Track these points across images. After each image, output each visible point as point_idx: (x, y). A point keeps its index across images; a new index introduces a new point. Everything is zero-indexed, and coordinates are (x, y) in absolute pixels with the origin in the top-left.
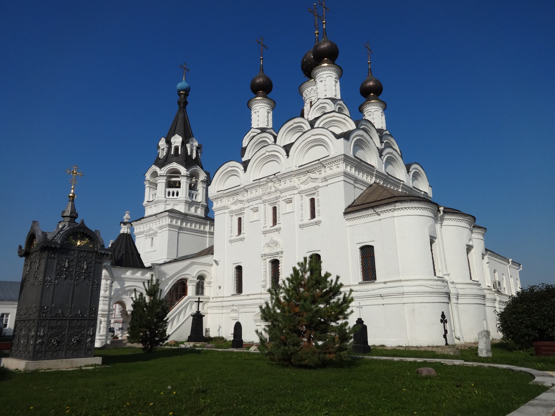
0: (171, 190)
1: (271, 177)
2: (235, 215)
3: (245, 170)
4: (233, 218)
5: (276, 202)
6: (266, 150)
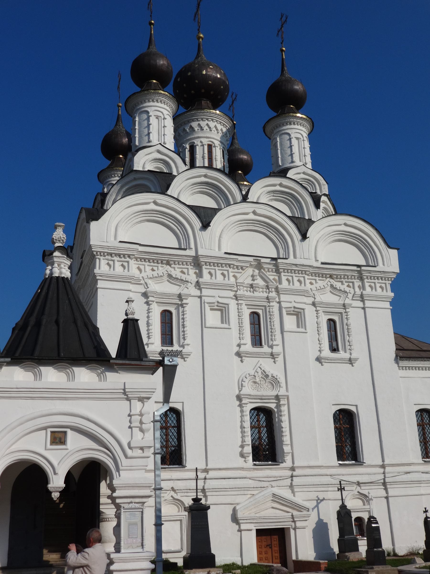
1: (263, 260)
3: (205, 226)
4: (152, 307)
5: (265, 306)
6: (252, 210)
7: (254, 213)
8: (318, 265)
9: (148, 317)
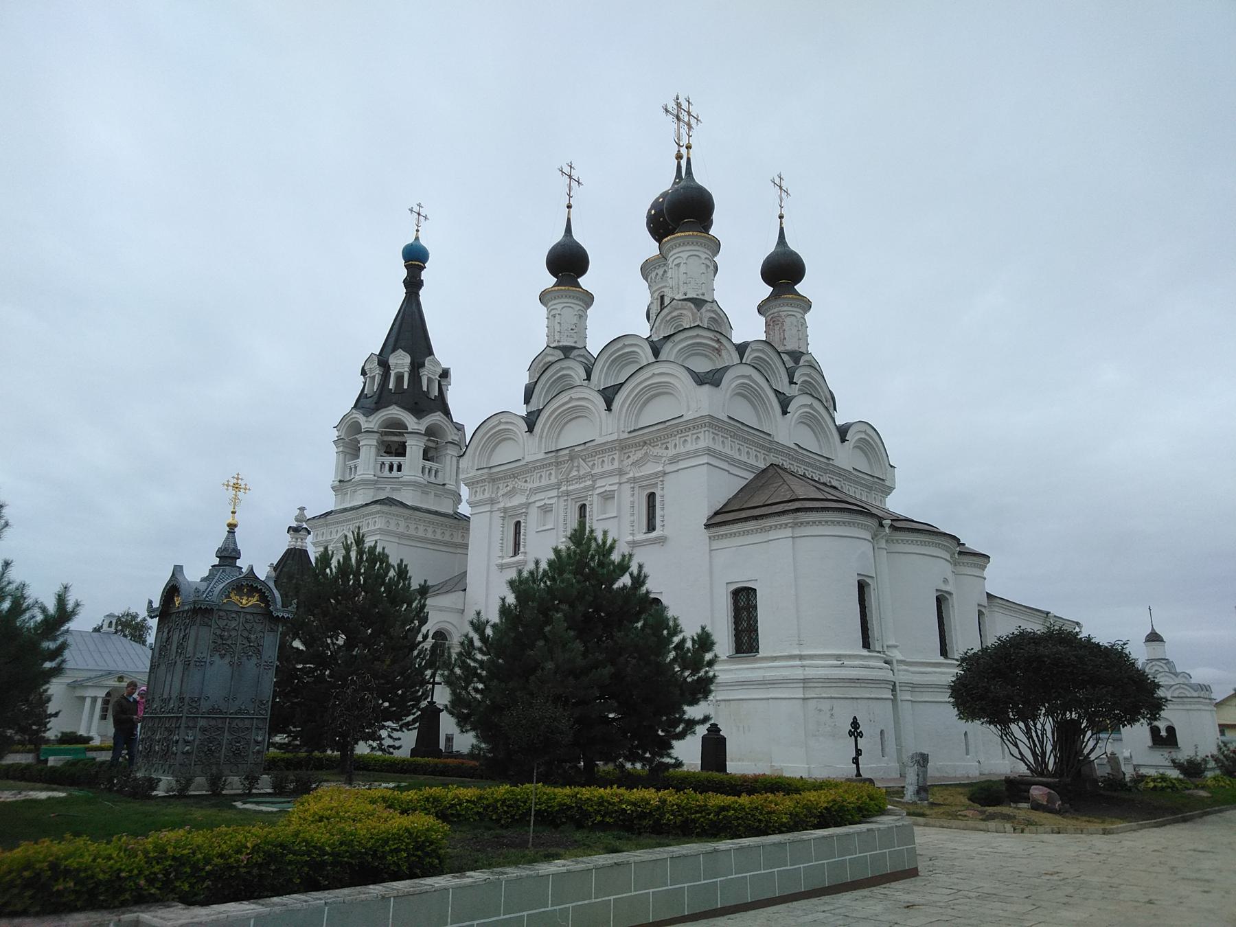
0: (388, 459)
1: (577, 449)
6: (569, 396)
8: (626, 435)
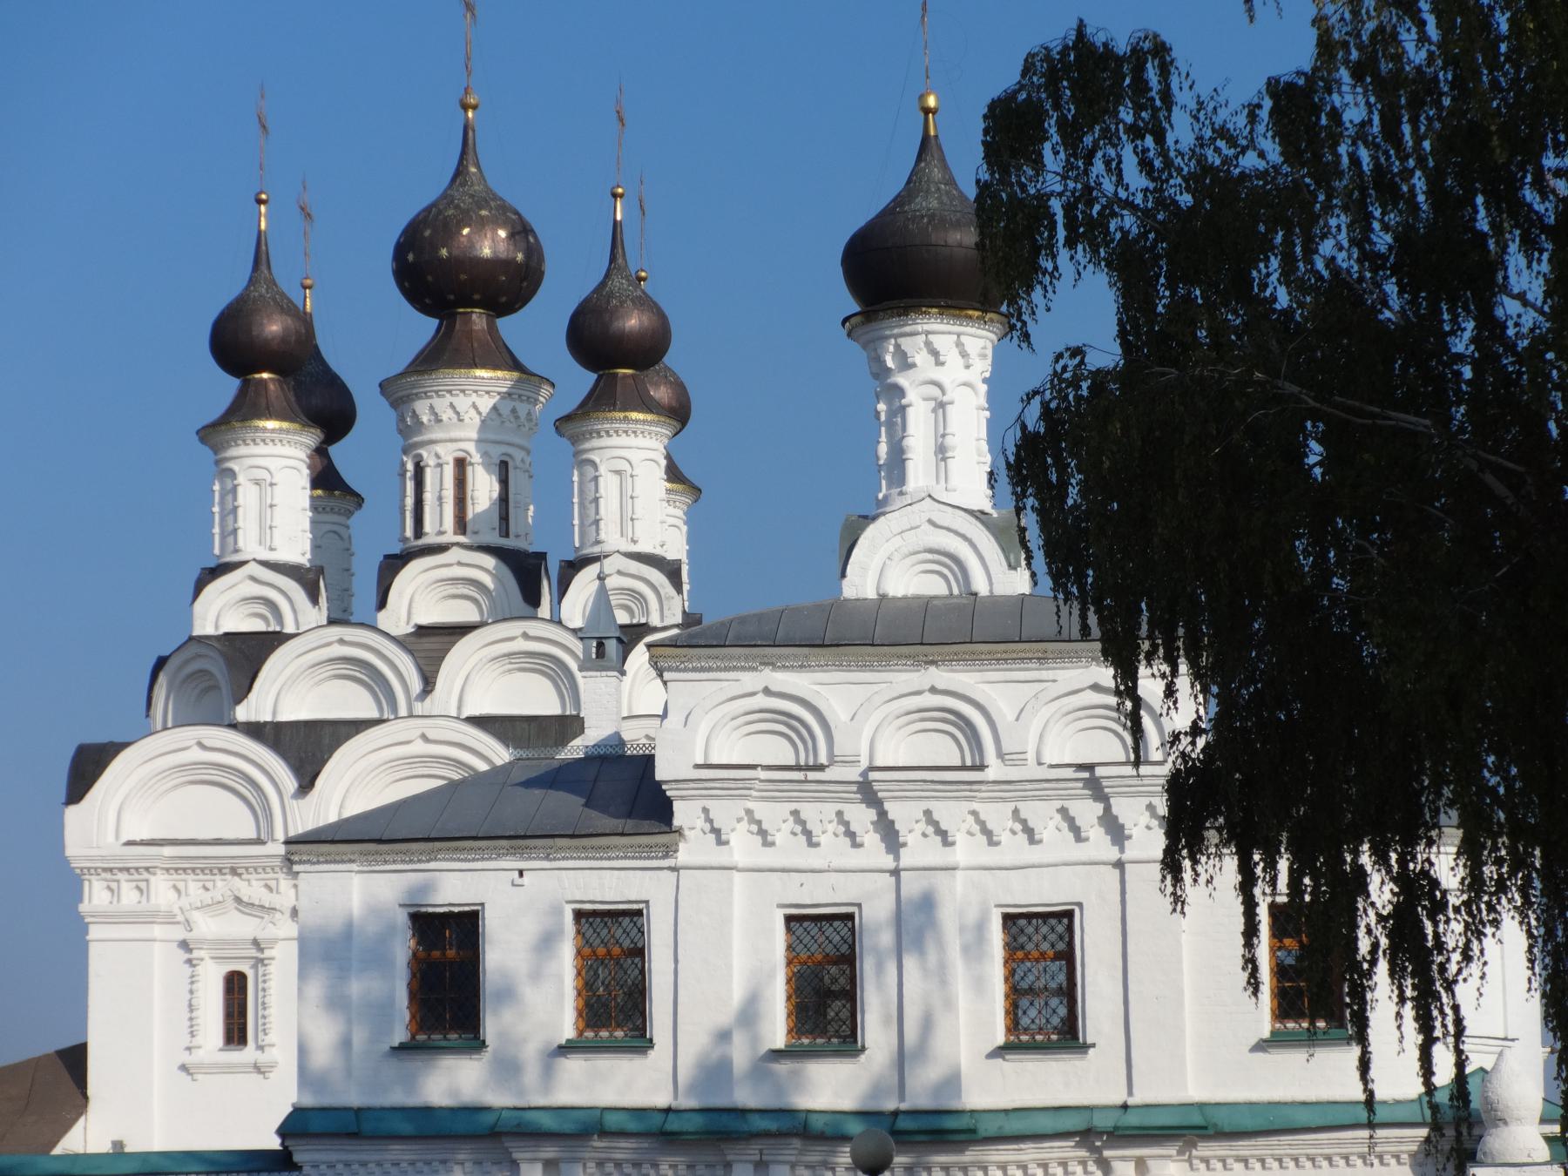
2: (213, 958)
6: (419, 733)
7: (424, 738)
9: (191, 992)
